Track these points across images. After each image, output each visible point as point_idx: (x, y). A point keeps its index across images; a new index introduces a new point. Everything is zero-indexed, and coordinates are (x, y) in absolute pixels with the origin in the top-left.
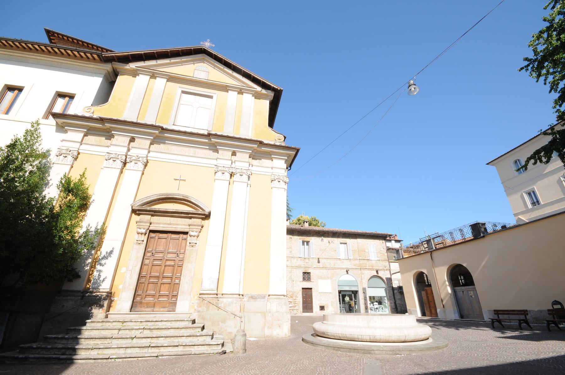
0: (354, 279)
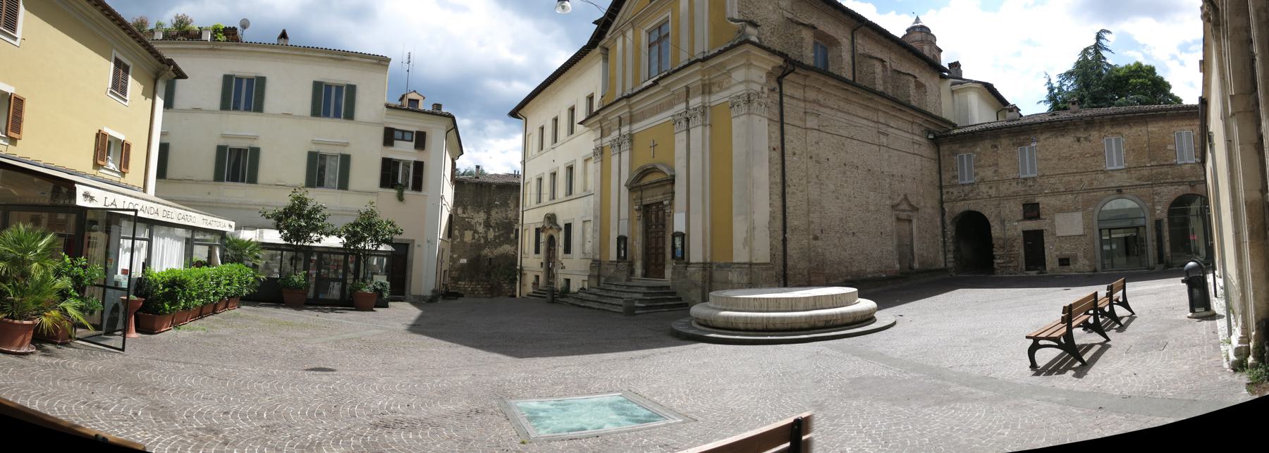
0: (1136, 206)
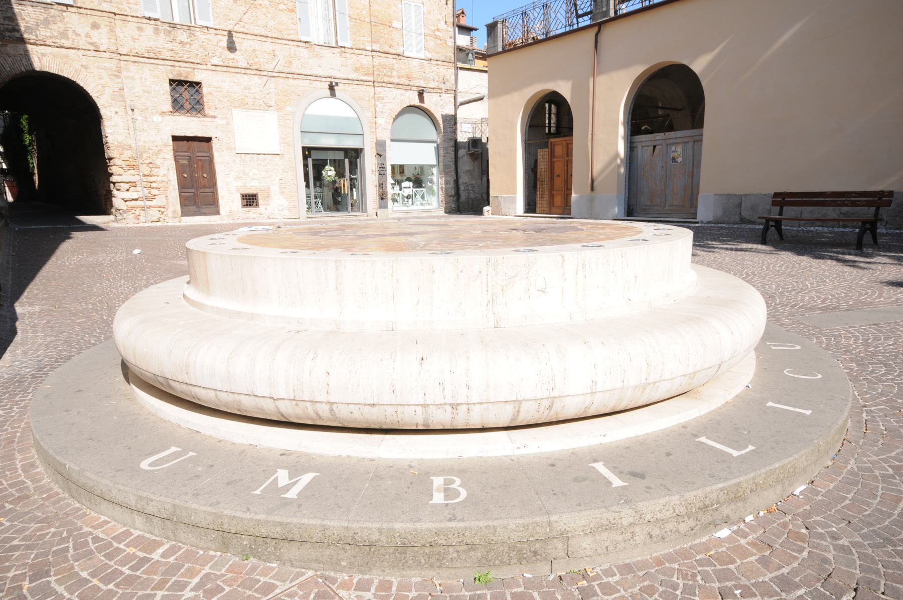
0: (351, 114)
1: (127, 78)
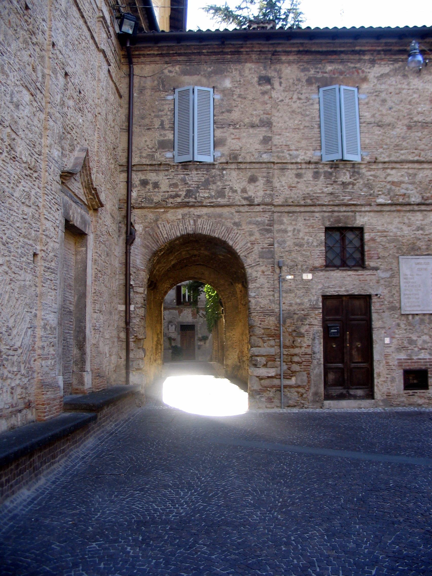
1: (279, 231)
